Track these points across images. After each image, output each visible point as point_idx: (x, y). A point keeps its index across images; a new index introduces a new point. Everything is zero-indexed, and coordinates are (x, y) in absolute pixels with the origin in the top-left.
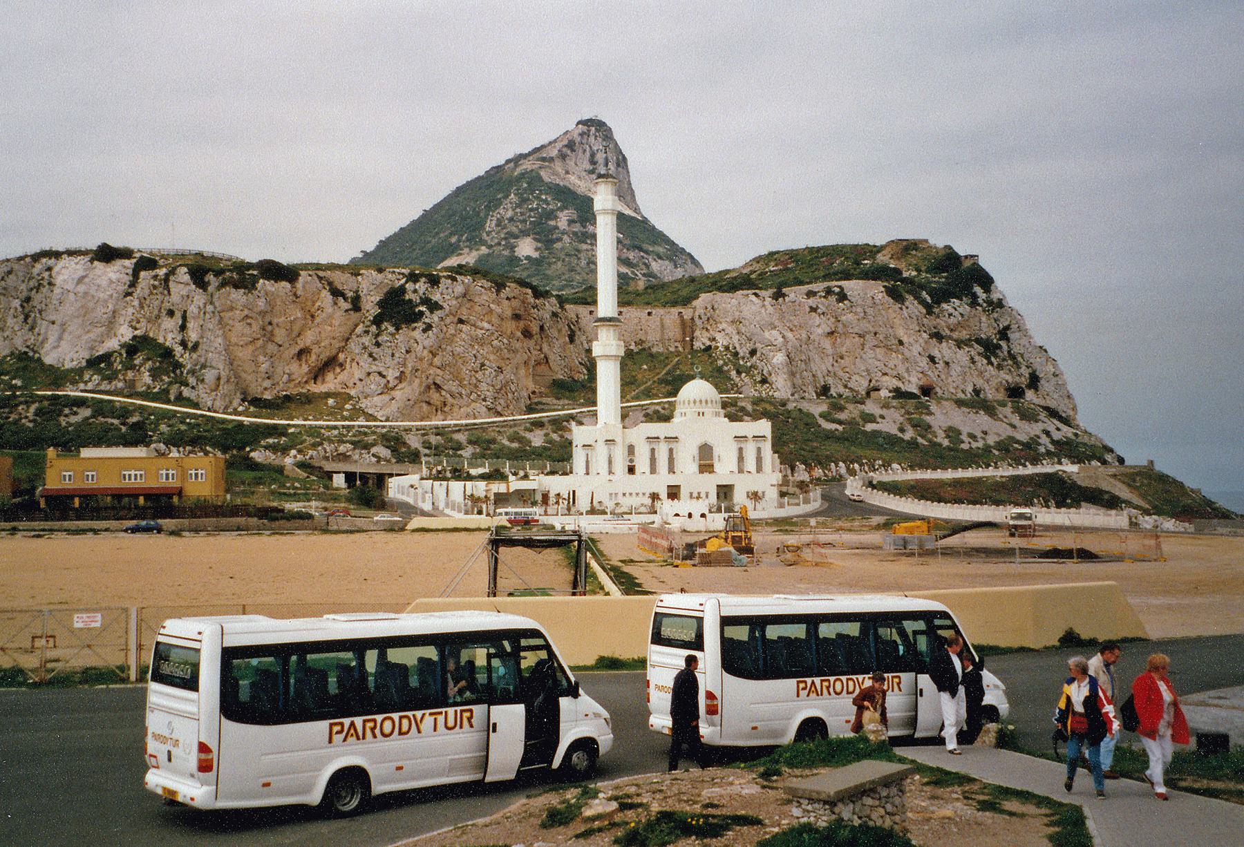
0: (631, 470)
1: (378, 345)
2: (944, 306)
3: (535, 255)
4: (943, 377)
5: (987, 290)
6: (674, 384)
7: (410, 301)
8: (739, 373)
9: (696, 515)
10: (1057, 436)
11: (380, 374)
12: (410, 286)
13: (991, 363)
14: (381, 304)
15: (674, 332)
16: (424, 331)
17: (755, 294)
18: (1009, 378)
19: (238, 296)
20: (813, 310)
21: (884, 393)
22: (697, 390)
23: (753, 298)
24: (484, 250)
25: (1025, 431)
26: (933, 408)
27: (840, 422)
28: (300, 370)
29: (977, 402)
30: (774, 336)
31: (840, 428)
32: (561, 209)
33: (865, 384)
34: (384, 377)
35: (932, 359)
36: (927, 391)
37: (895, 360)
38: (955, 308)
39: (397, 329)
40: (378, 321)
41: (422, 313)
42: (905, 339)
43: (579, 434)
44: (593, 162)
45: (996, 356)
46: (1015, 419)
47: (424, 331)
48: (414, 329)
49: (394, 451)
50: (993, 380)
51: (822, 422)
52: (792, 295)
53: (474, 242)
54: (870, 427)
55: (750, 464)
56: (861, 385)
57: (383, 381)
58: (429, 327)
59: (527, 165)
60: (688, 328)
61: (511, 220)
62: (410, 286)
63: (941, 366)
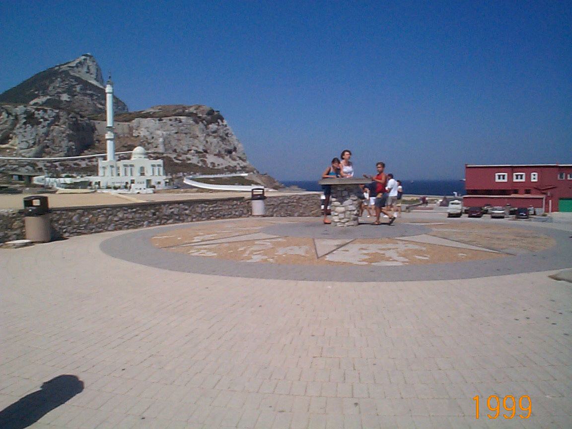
3: (68, 100)
6: (131, 148)
7: (37, 118)
9: (143, 188)
10: (242, 165)
11: (26, 141)
12: (36, 112)
15: (126, 131)
16: (43, 128)
20: (171, 125)
21: (192, 151)
22: (138, 150)
23: (153, 121)
24: (48, 97)
25: (233, 163)
27: (180, 160)
29: (219, 155)
30: (159, 132)
31: (180, 162)
32: (78, 84)
34: (28, 143)
35: (207, 142)
36: (206, 151)
37: (196, 141)
38: (213, 127)
39: (33, 127)
40: (25, 124)
41: (41, 122)
43: (101, 163)
44: (88, 68)
46: (230, 160)
48: (39, 127)
49: (34, 168)
51: (174, 160)
52: (164, 121)
53: (45, 94)
54: (189, 162)
55: (156, 173)
56: (186, 149)
58: (44, 127)
59: (64, 68)
60: (131, 129)
61: (59, 87)
63: (209, 143)
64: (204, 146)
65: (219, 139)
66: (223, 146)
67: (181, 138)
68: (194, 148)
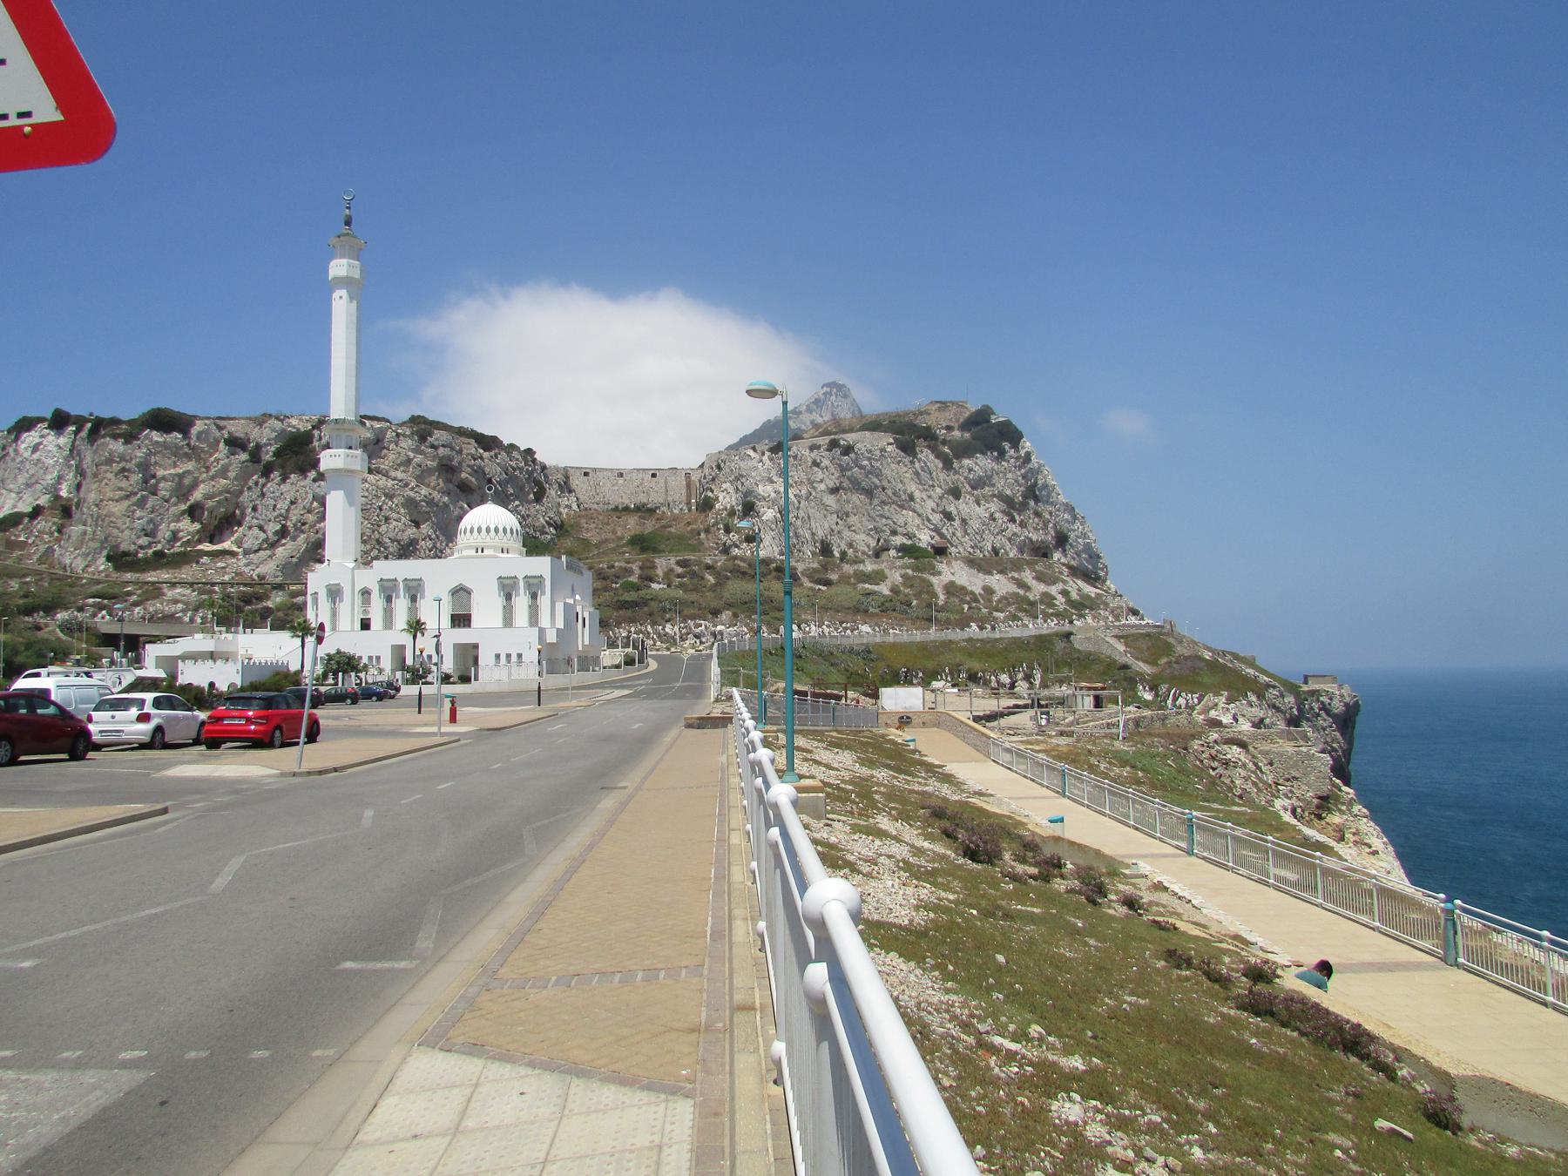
0: (365, 625)
1: (263, 495)
2: (966, 462)
4: (959, 534)
5: (1015, 446)
8: (728, 530)
11: (261, 528)
12: (316, 433)
13: (1013, 520)
14: (278, 454)
16: (314, 480)
17: (754, 449)
18: (1034, 538)
19: (118, 446)
20: (816, 464)
21: (893, 553)
23: (751, 453)
26: (940, 567)
28: (188, 527)
33: (873, 543)
35: (948, 516)
36: (940, 551)
38: (981, 464)
39: (284, 480)
42: (917, 494)
45: (1020, 512)
47: (314, 480)
50: (1007, 536)
52: (794, 449)
57: (263, 536)
62: (316, 433)
63: (957, 523)
64: (937, 530)
65: (995, 506)
66: (1013, 528)
67: (848, 508)
68: (899, 540)
